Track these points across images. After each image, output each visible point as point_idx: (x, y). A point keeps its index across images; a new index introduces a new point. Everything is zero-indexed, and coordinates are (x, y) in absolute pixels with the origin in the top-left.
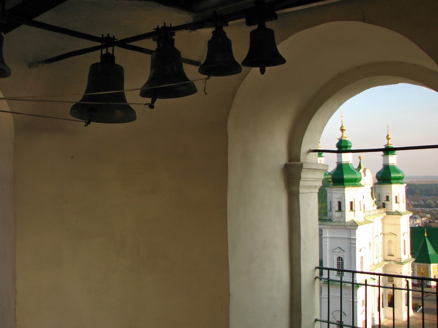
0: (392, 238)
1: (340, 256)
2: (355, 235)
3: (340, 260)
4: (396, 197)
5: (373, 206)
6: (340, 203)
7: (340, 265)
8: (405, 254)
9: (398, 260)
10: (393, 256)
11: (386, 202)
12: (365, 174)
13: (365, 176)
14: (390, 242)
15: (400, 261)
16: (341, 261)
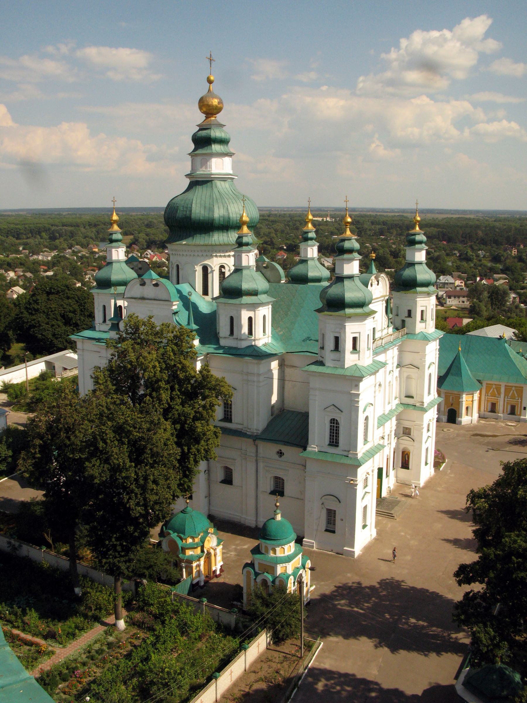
0: (413, 372)
1: (336, 418)
2: (358, 389)
3: (334, 423)
4: (422, 311)
5: (388, 326)
6: (337, 339)
7: (333, 430)
8: (429, 393)
9: (418, 404)
10: (412, 397)
11: (408, 320)
12: (378, 282)
13: (378, 284)
14: (408, 378)
15: (422, 406)
16: (335, 425)
